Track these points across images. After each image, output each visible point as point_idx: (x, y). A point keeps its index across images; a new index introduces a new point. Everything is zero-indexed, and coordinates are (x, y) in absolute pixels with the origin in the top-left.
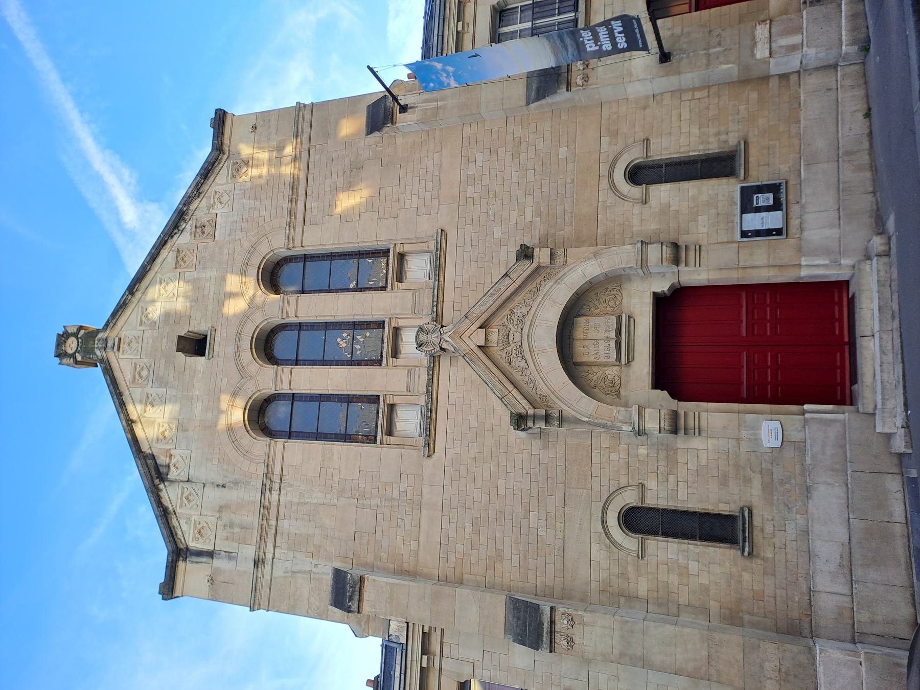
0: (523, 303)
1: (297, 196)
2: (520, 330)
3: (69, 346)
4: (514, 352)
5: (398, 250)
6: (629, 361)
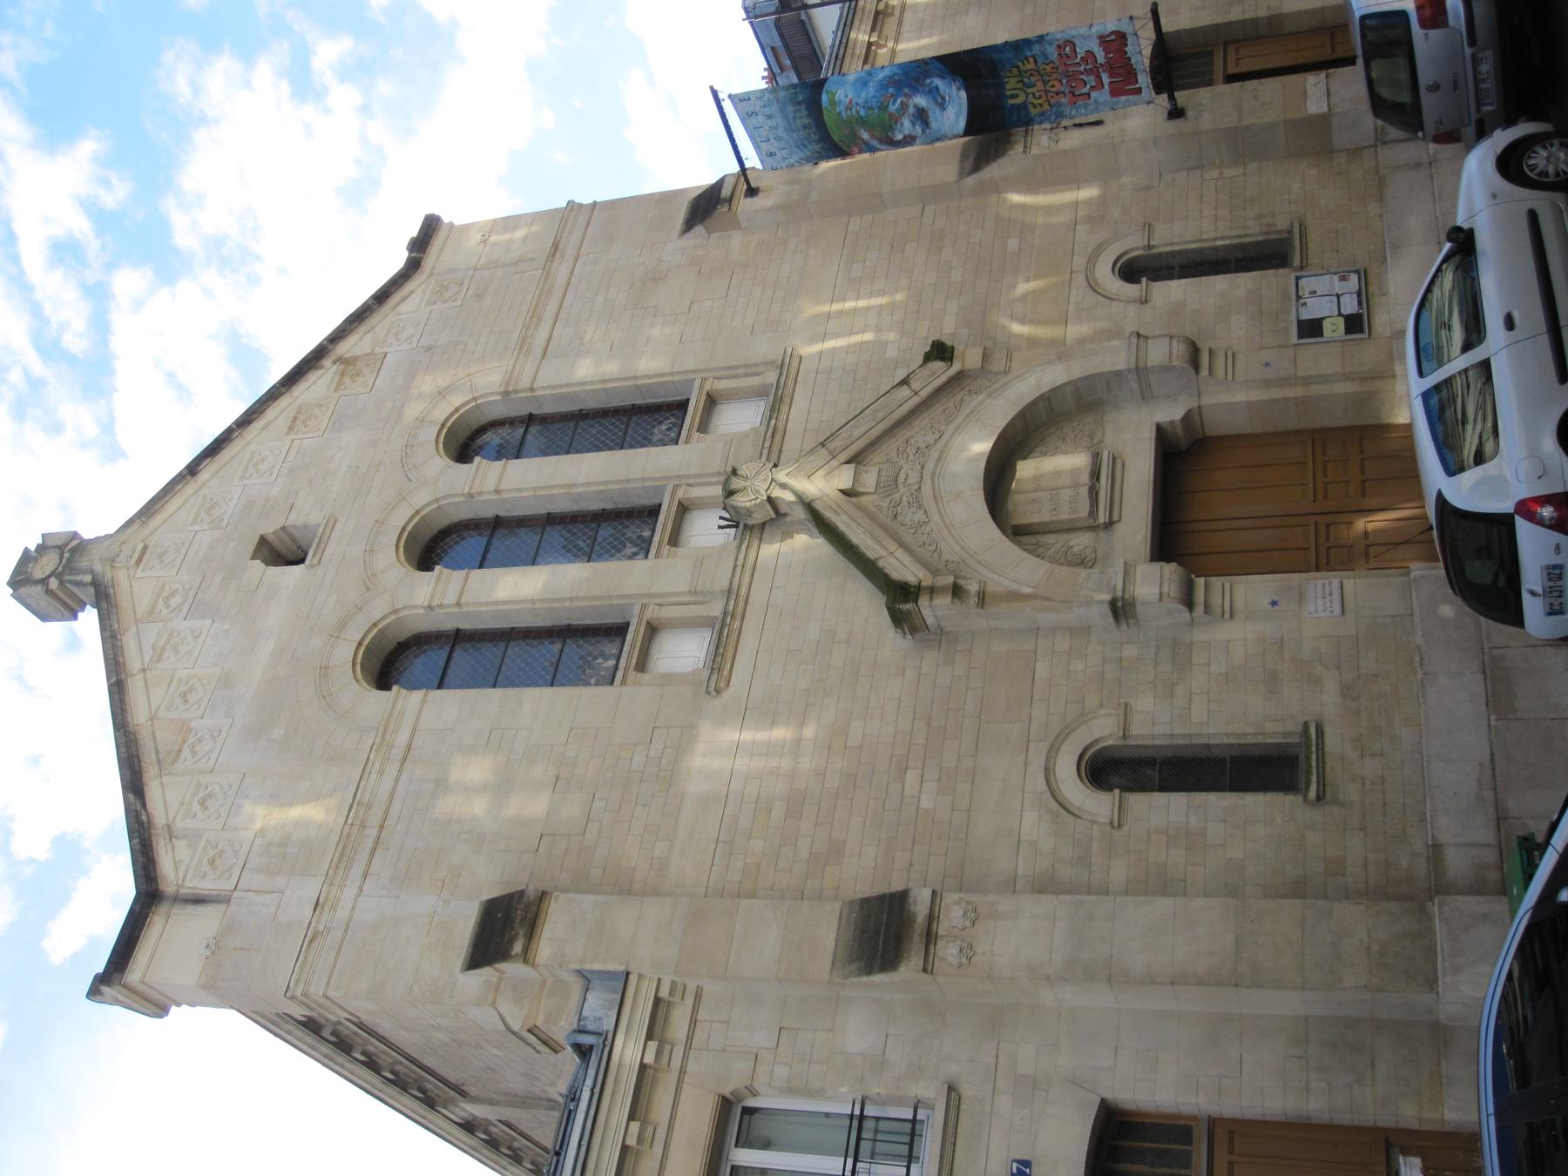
1: (540, 319)
2: (919, 467)
3: (42, 568)
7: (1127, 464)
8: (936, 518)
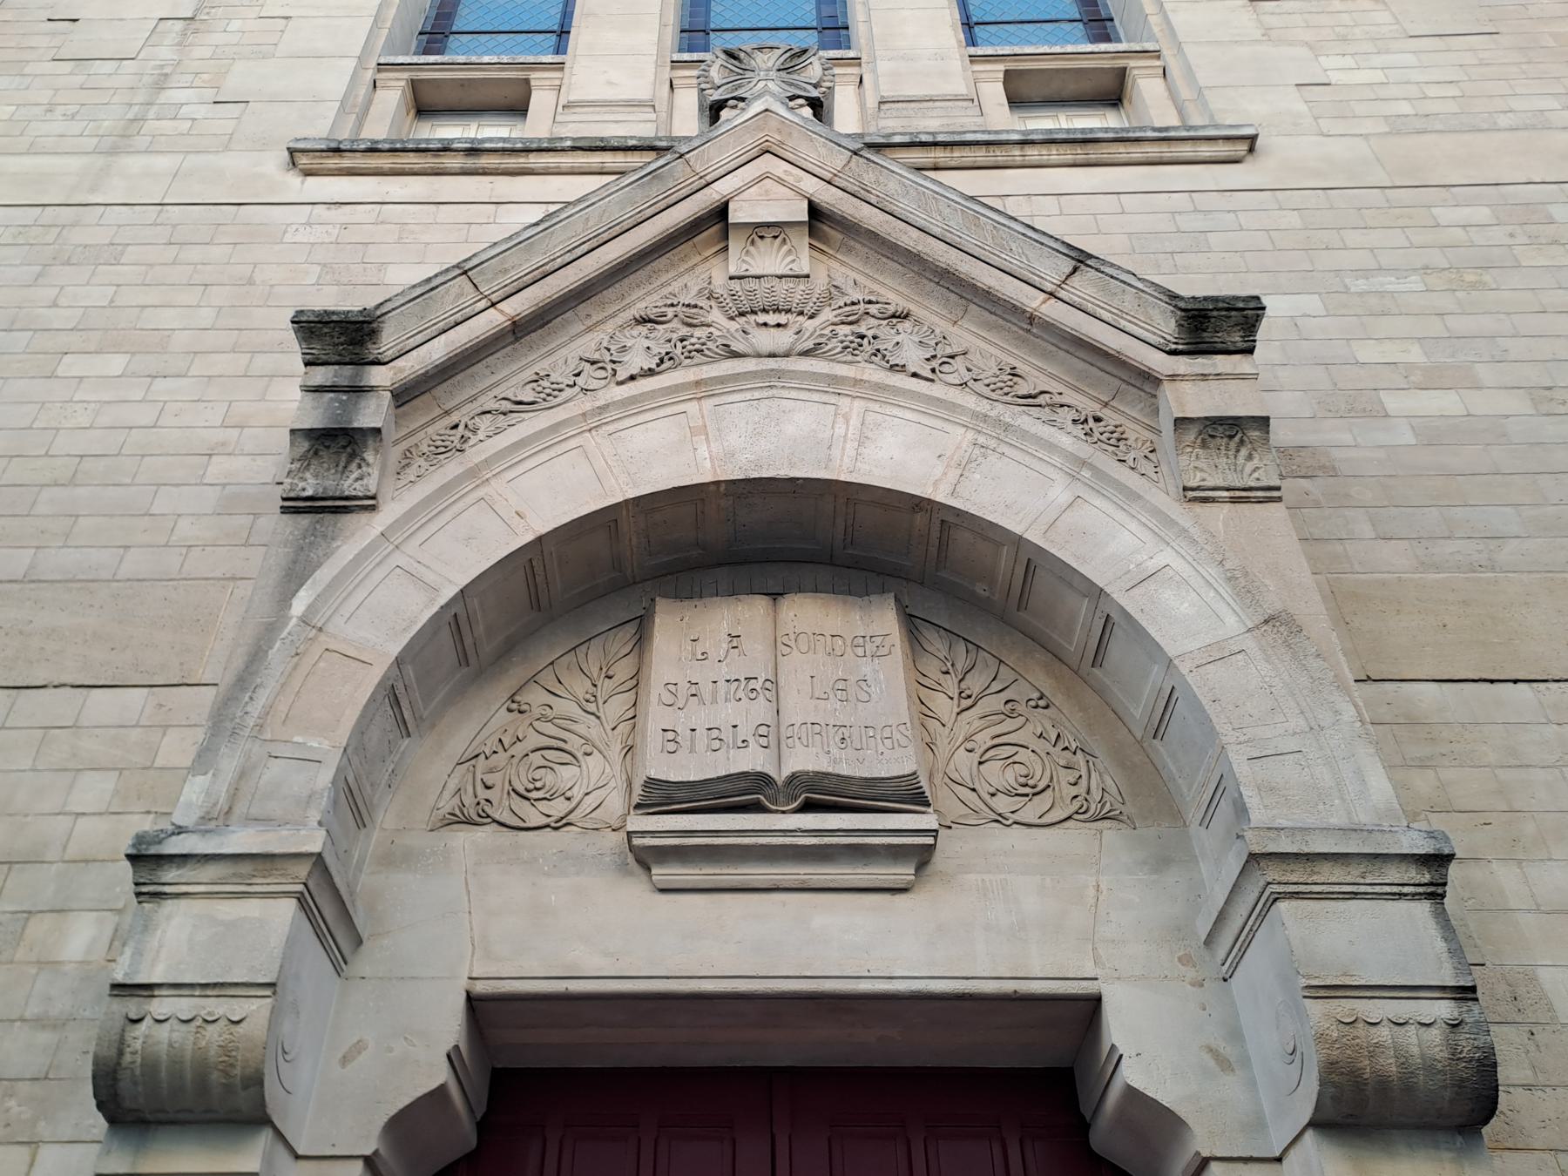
0: (949, 351)
4: (699, 332)
6: (645, 858)
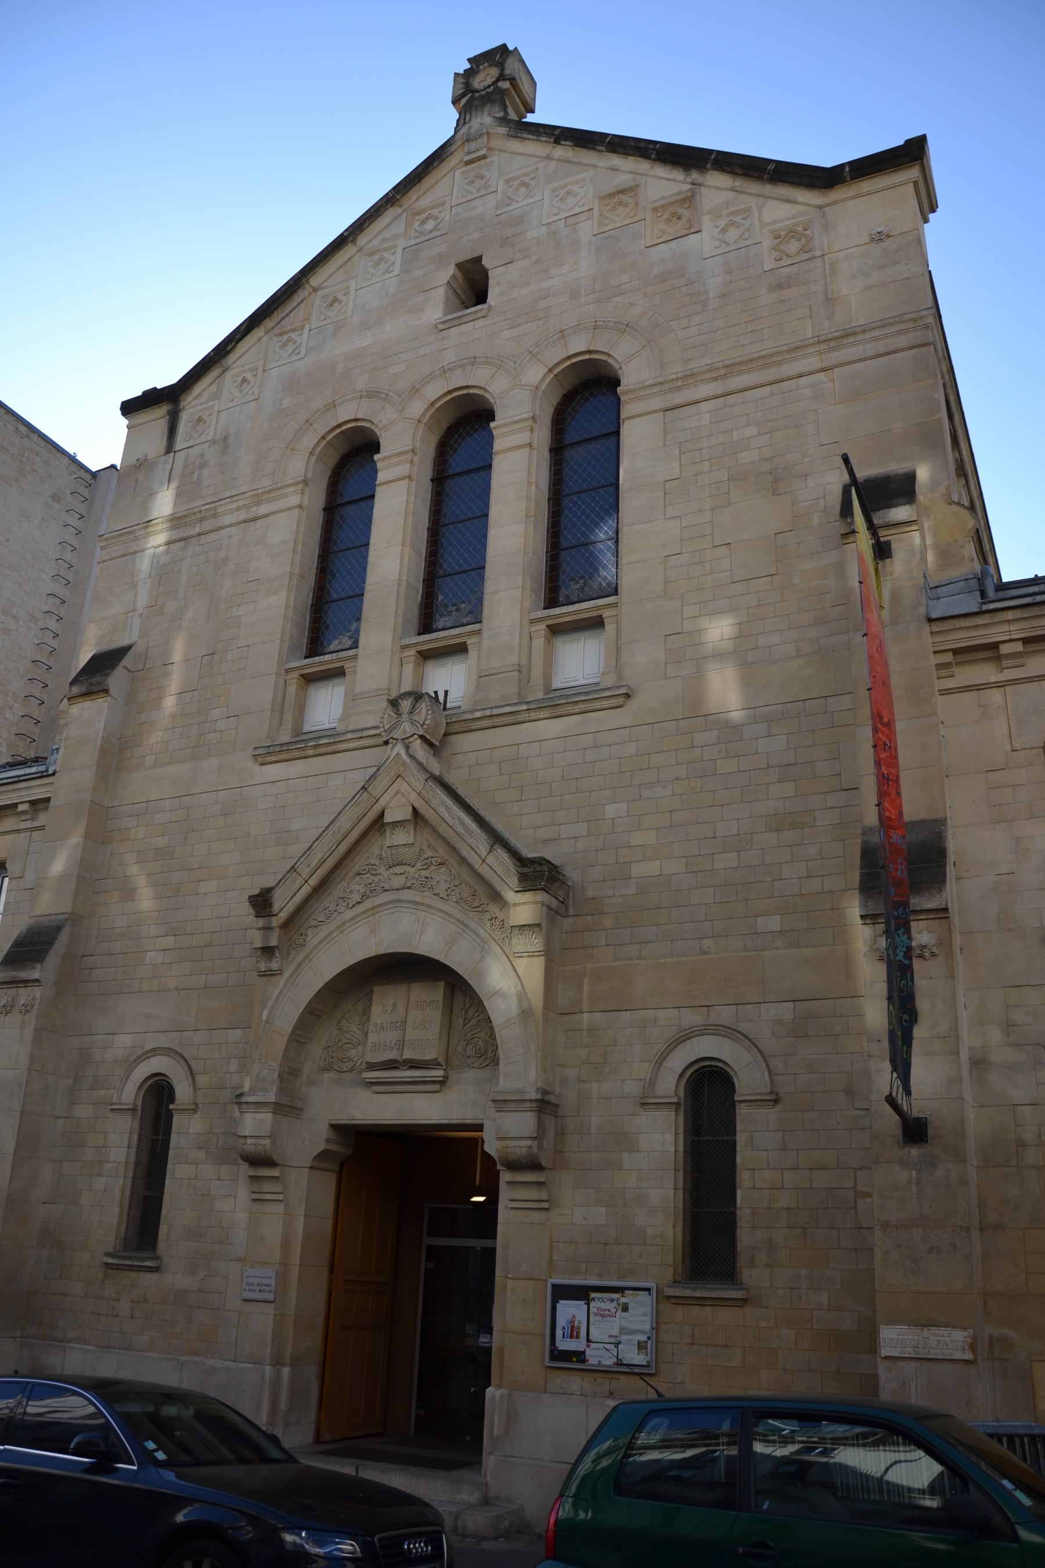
1: (725, 377)
2: (409, 884)
4: (376, 879)
5: (606, 614)
7: (437, 1094)
8: (349, 914)
